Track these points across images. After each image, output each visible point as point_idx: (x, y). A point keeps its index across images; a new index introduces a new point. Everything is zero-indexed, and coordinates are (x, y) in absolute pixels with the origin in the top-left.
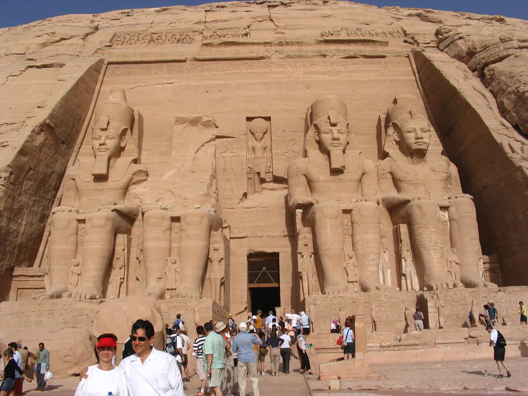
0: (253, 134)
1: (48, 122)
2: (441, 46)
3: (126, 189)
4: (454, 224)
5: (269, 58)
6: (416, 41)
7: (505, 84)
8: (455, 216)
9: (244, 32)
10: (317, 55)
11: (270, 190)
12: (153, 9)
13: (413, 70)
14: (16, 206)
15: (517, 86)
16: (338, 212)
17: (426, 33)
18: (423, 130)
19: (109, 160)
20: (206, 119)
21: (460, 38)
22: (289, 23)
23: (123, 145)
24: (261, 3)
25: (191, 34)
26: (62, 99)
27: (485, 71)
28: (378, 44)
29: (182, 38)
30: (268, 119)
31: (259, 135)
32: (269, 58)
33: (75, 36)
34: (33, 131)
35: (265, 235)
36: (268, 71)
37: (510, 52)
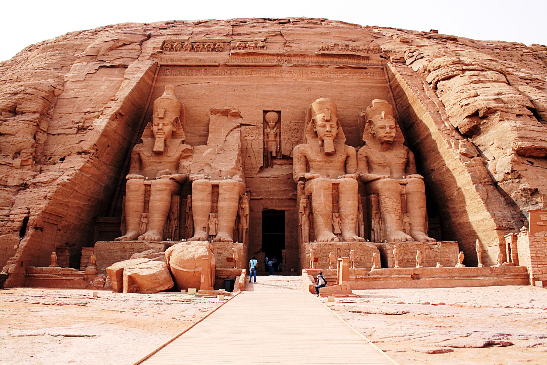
1: (120, 111)
5: (281, 66)
15: (459, 100)
17: (397, 50)
18: (391, 128)
19: (165, 140)
21: (422, 58)
22: (295, 38)
23: (175, 130)
25: (222, 44)
27: (438, 85)
29: (215, 48)
30: (279, 112)
32: (281, 66)
33: (134, 42)
35: (275, 197)
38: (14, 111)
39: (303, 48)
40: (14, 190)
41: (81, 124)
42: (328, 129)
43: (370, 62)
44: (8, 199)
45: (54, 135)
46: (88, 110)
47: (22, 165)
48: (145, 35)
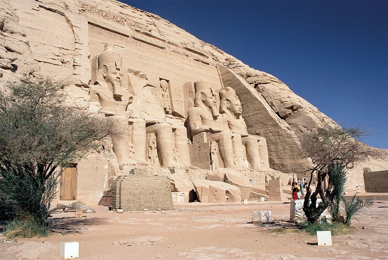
0: (161, 87)
2: (230, 66)
3: (127, 106)
4: (261, 148)
6: (218, 60)
7: (272, 95)
8: (262, 145)
9: (149, 30)
11: (170, 118)
13: (219, 74)
20: (141, 73)
21: (240, 66)
24: (141, 11)
27: (259, 86)
30: (168, 81)
36: (165, 55)
37: (270, 81)
39: (172, 40)
45: (40, 62)
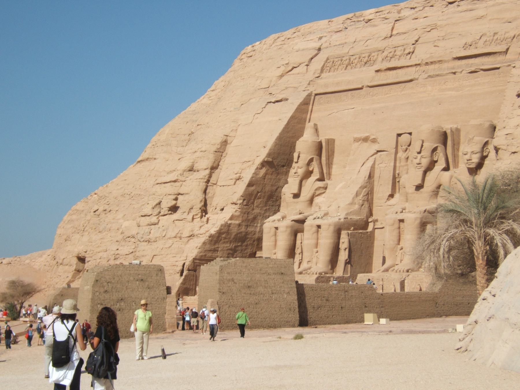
1: (266, 160)
3: (311, 201)
5: (417, 79)
10: (450, 73)
12: (369, 13)
14: (251, 217)
16: (394, 221)
19: (301, 182)
23: (311, 169)
26: (276, 140)
28: (498, 54)
30: (410, 134)
31: (404, 148)
32: (417, 79)
33: (302, 63)
34: (257, 168)
38: (191, 169)
40: (186, 239)
41: (238, 175)
42: (417, 161)
43: (509, 56)
44: (181, 248)
46: (246, 159)
47: (193, 219)
48: (315, 49)
